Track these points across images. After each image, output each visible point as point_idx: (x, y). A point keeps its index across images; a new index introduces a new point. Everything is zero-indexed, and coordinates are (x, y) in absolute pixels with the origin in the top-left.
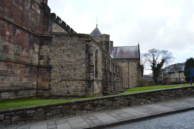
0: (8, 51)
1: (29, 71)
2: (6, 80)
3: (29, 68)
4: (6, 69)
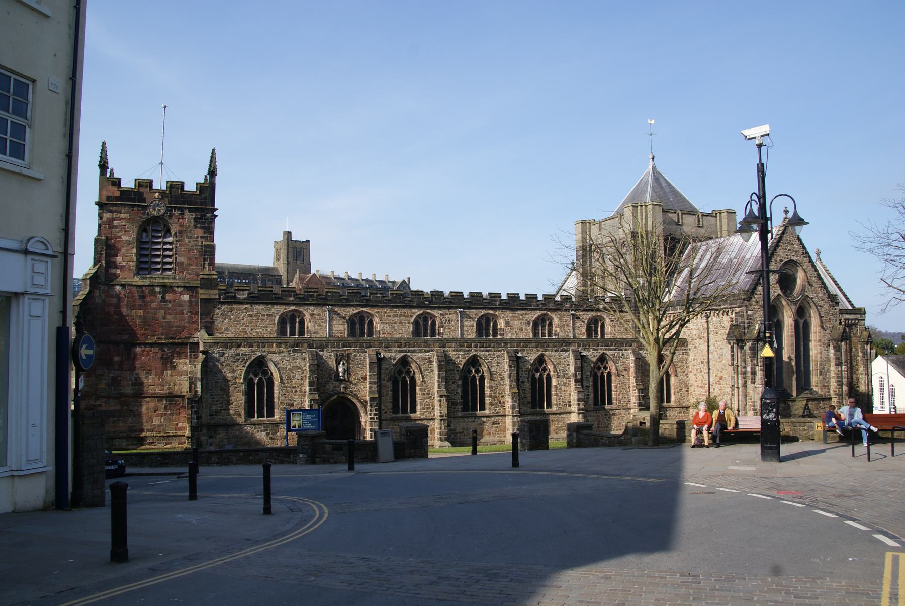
0: (120, 383)
1: (166, 407)
2: (121, 422)
3: (164, 402)
4: (118, 407)
